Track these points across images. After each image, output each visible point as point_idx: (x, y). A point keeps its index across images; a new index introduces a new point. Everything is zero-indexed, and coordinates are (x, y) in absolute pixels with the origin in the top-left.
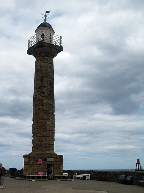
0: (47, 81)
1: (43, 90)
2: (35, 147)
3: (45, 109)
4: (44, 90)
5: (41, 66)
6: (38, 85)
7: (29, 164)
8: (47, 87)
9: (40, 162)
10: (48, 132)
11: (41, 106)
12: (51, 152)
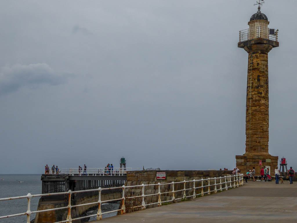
0: (264, 81)
1: (259, 90)
2: (250, 147)
3: (262, 110)
4: (261, 90)
5: (258, 64)
7: (245, 165)
8: (264, 87)
9: (261, 163)
10: (265, 133)
11: (258, 107)
12: (265, 153)
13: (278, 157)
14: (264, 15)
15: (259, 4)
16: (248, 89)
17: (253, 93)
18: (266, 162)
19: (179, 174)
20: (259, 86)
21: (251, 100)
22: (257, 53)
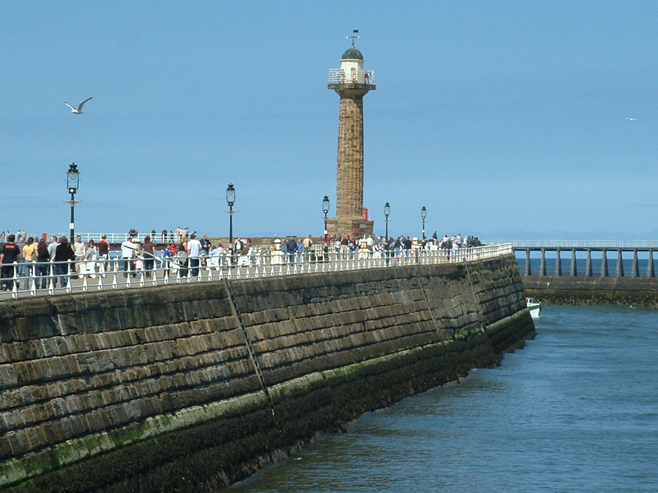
6: (347, 136)
13: (373, 222)
14: (359, 52)
16: (340, 140)
17: (346, 146)
19: (264, 242)
20: (353, 138)
21: (343, 154)
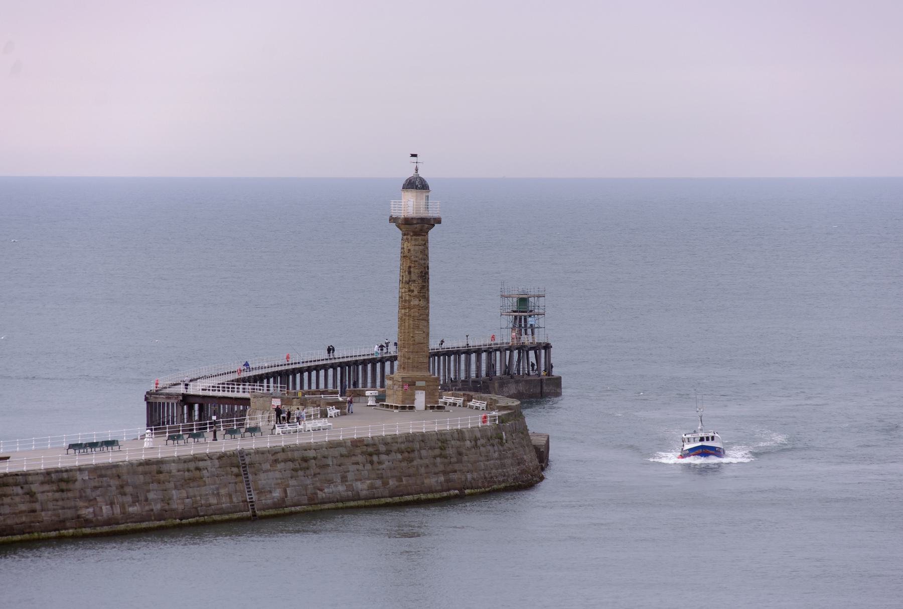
1: (410, 287)
5: (409, 250)
6: (404, 279)
8: (417, 283)
15: (417, 163)
18: (416, 385)
22: (407, 235)
